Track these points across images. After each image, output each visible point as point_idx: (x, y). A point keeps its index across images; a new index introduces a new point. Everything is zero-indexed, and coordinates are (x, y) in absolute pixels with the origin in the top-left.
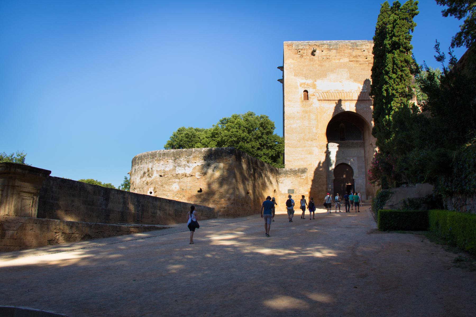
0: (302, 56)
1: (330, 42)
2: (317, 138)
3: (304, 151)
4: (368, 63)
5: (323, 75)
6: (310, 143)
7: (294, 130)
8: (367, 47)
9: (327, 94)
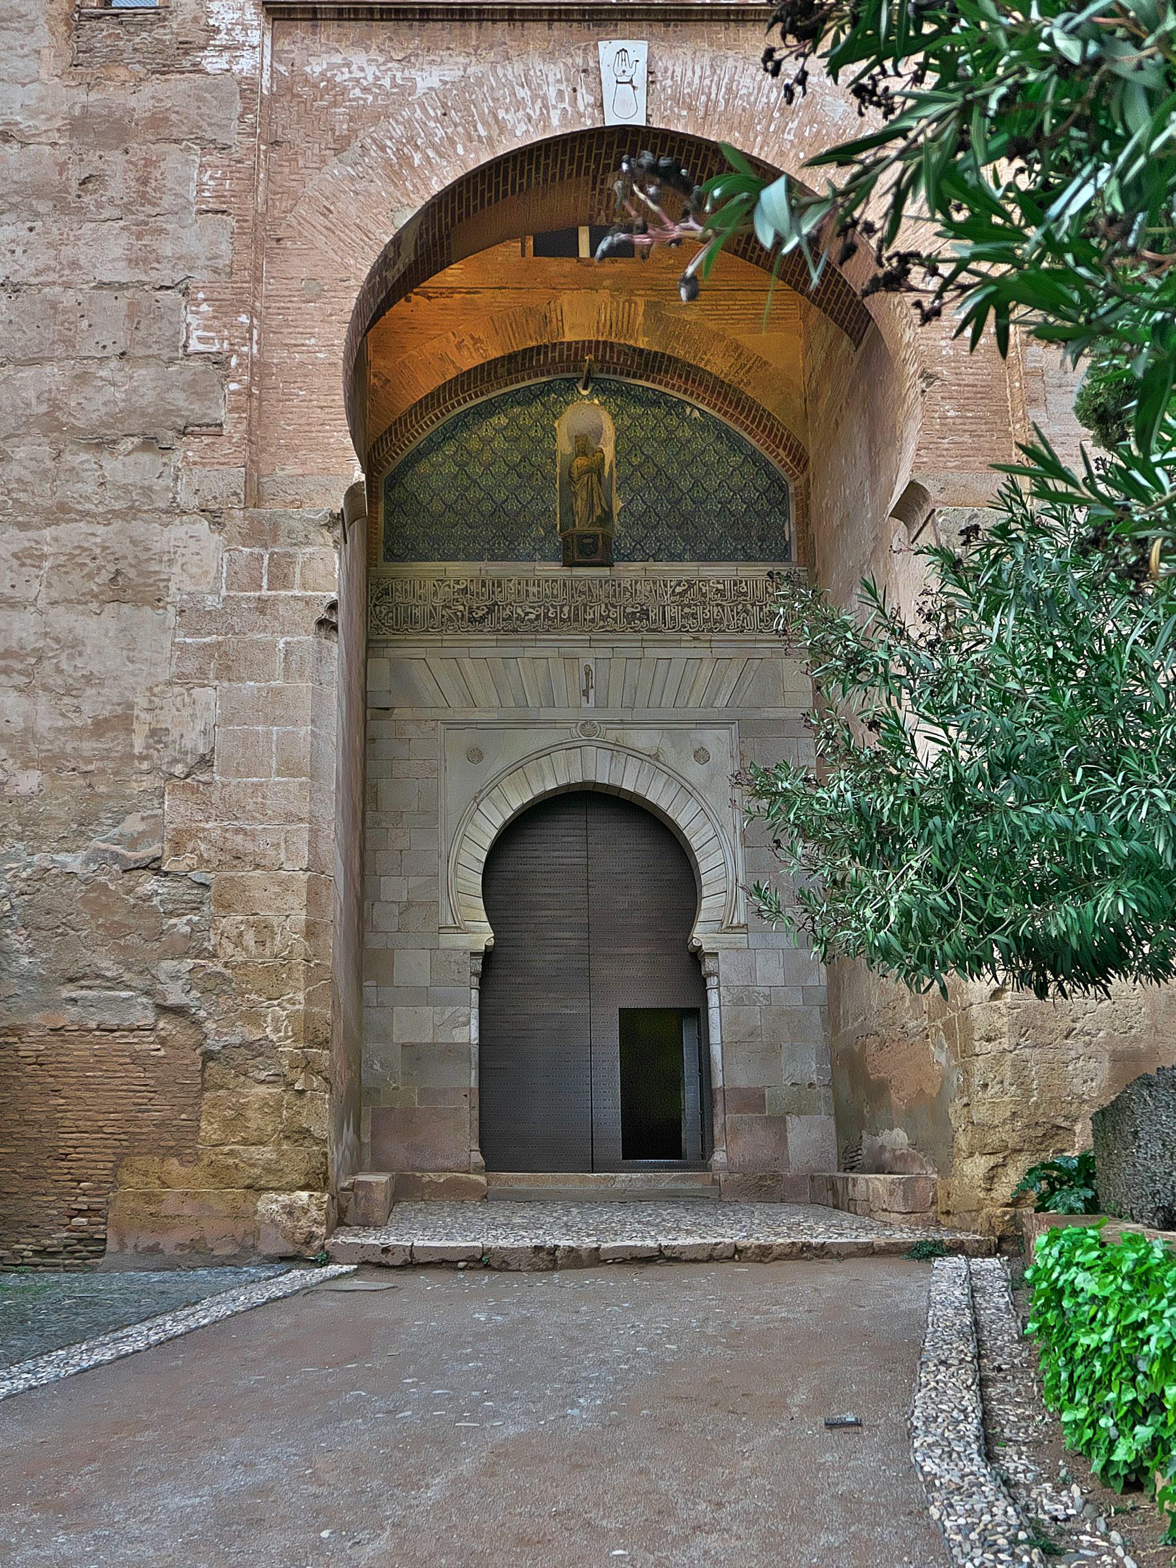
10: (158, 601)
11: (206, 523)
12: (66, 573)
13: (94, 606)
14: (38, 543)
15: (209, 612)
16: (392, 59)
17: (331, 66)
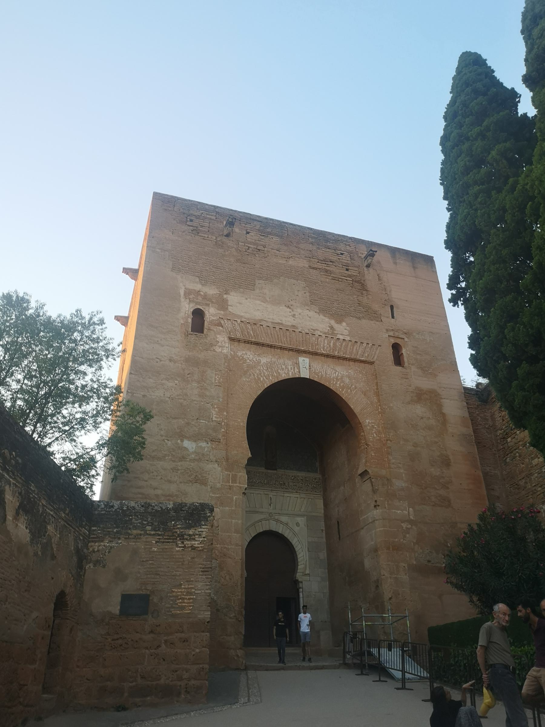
2: (220, 437)
3: (179, 472)
4: (351, 279)
11: (217, 465)
12: (184, 475)
13: (191, 484)
14: (177, 466)
15: (218, 488)
16: (256, 354)
17: (243, 354)
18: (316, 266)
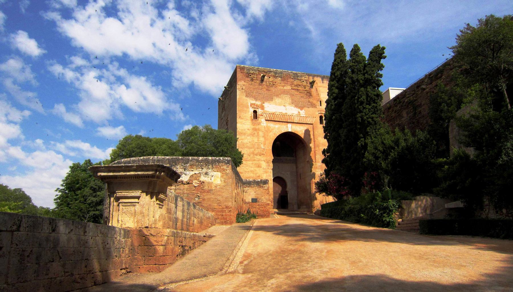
0: (252, 80)
1: (276, 70)
2: (264, 153)
5: (270, 99)
6: (258, 157)
7: (245, 145)
8: (306, 79)
9: (273, 115)
10: (261, 167)
18: (294, 88)
